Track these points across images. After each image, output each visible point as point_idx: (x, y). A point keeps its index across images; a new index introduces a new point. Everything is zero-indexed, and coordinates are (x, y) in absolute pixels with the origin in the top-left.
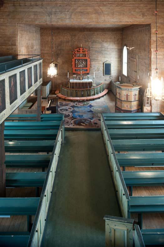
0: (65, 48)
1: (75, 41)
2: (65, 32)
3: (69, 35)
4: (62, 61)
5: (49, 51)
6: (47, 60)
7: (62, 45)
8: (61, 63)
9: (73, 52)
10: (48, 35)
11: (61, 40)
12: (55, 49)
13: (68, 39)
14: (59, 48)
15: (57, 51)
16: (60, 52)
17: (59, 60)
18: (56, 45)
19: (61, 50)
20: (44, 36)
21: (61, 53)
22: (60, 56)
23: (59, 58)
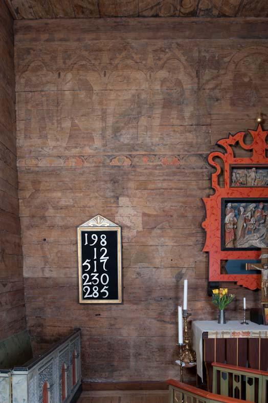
0: (156, 140)
1: (219, 95)
2: (160, 43)
3: (183, 58)
4: (144, 214)
5: (67, 158)
6: (55, 208)
7: (143, 121)
8: (140, 229)
9: (210, 159)
10: (60, 61)
11: (133, 90)
12: (98, 143)
13: (179, 83)
14: (126, 138)
15: (112, 157)
16: (127, 162)
17: (121, 211)
18: (103, 119)
19: (132, 148)
20: (37, 69)
21: (133, 166)
22: (131, 185)
23: (123, 200)
